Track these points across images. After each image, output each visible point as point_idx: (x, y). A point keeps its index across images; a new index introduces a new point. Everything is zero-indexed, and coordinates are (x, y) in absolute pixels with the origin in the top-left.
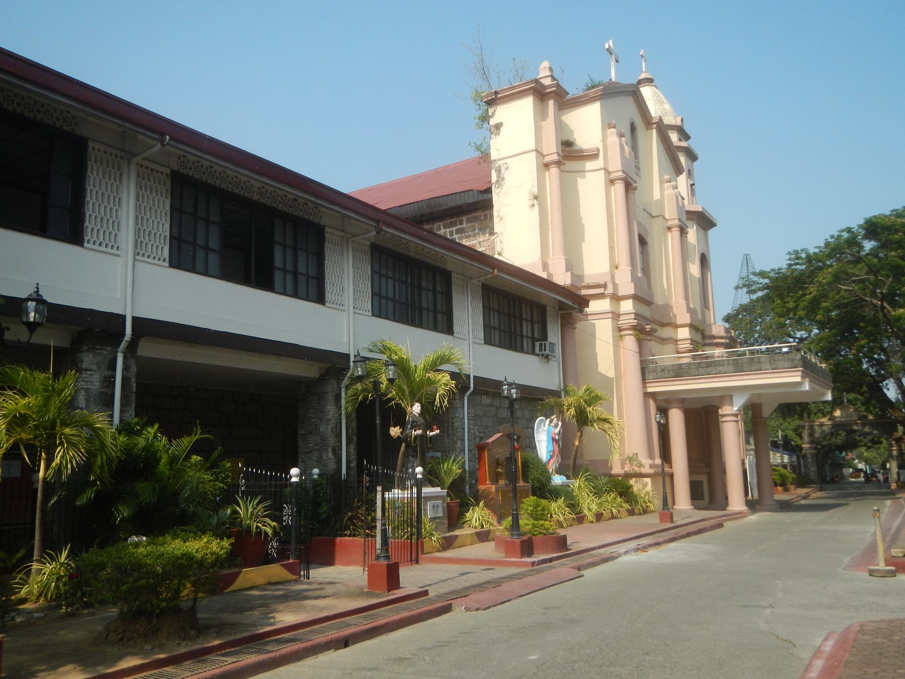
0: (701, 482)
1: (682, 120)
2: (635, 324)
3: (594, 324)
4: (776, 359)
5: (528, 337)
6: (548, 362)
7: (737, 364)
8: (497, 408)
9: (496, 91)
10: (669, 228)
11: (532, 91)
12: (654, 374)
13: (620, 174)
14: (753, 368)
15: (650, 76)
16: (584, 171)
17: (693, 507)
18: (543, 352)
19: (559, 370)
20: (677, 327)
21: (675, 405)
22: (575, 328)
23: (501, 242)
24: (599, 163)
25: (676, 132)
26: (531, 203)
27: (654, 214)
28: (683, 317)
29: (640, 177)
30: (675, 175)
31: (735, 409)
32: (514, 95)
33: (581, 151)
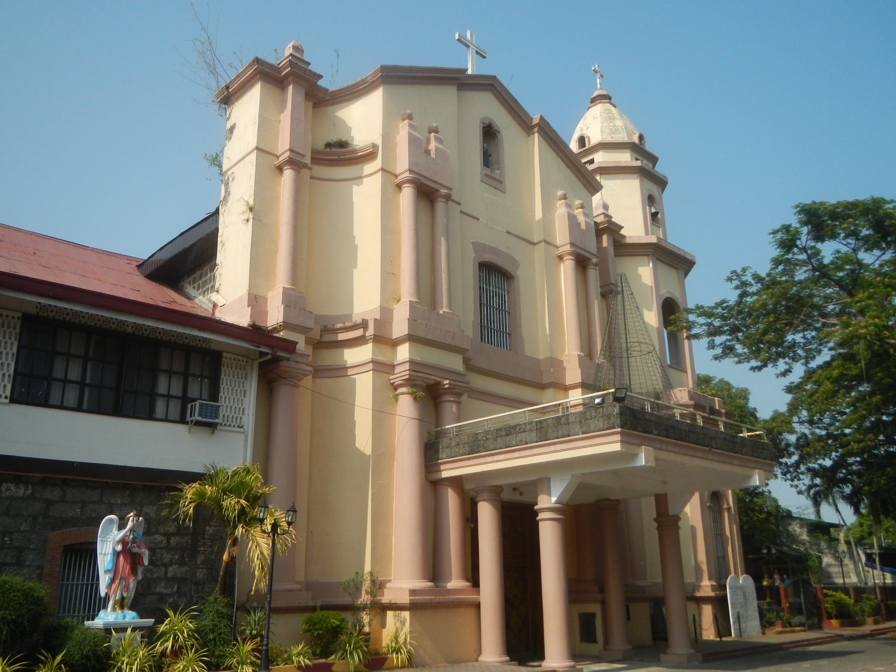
0: (593, 616)
1: (641, 137)
2: (407, 377)
3: (355, 380)
4: (588, 416)
5: (168, 397)
6: (213, 433)
7: (541, 428)
8: (50, 503)
9: (226, 86)
10: (561, 258)
11: (258, 76)
12: (448, 450)
13: (407, 174)
14: (560, 433)
15: (604, 92)
16: (361, 177)
17: (508, 658)
18: (193, 418)
19: (246, 446)
20: (566, 389)
21: (486, 495)
22: (296, 386)
23: (220, 275)
24: (377, 164)
25: (629, 151)
26: (245, 216)
27: (535, 241)
28: (573, 375)
29: (505, 193)
30: (585, 192)
31: (554, 499)
32: (244, 87)
33: (355, 151)
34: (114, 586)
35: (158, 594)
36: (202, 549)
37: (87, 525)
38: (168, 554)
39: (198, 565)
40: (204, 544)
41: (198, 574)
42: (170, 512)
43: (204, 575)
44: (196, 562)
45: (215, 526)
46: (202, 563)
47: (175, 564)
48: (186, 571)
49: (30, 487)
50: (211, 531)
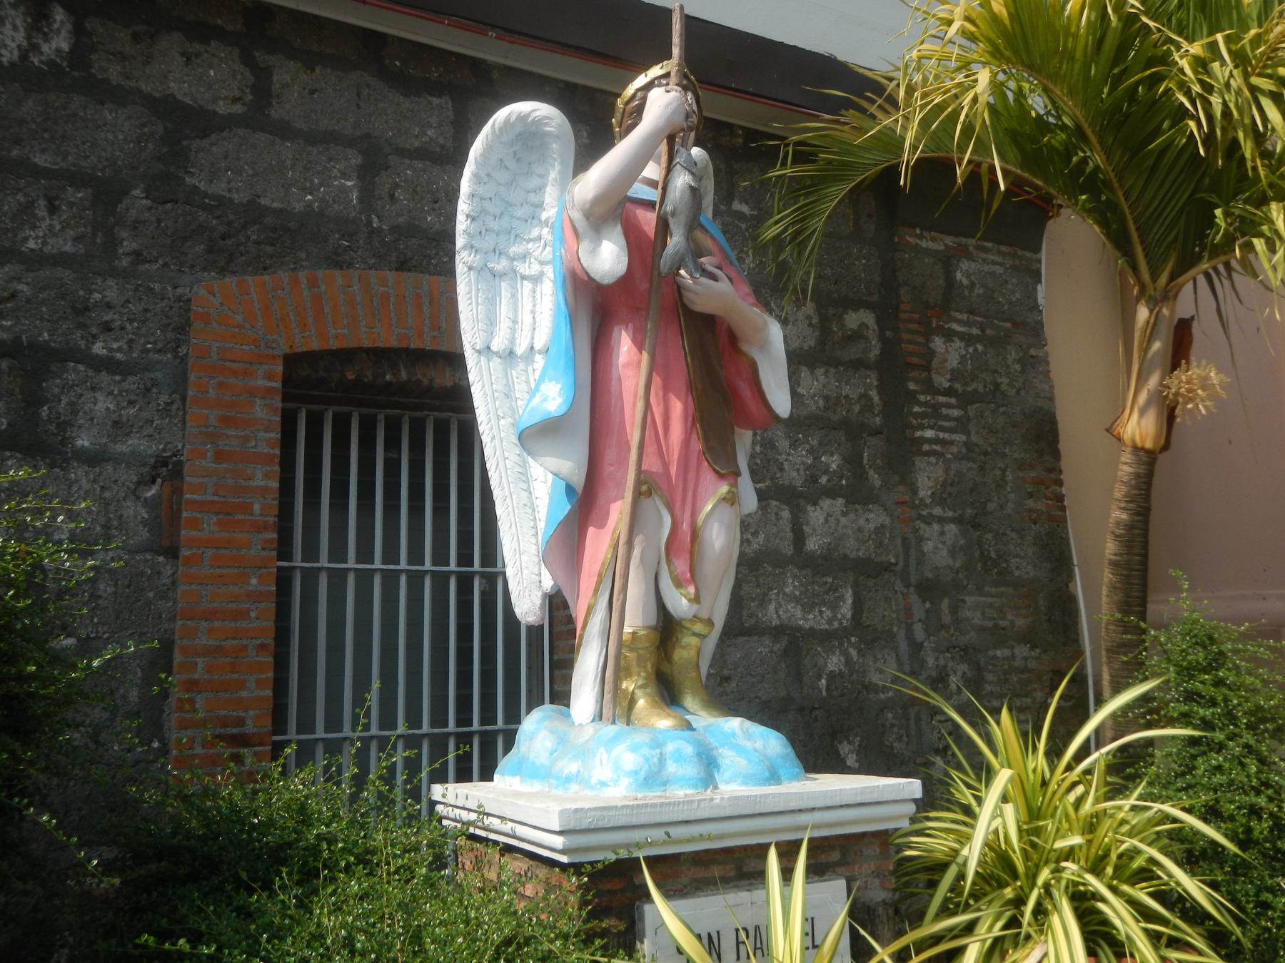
34: (598, 544)
35: (778, 631)
36: (929, 434)
37: (403, 265)
38: (794, 444)
39: (923, 504)
40: (935, 412)
41: (928, 546)
42: (803, 218)
43: (953, 553)
44: (914, 492)
45: (968, 339)
46: (939, 499)
47: (831, 493)
48: (880, 529)
49: (59, 15)
50: (953, 361)
